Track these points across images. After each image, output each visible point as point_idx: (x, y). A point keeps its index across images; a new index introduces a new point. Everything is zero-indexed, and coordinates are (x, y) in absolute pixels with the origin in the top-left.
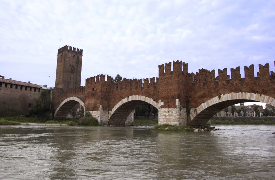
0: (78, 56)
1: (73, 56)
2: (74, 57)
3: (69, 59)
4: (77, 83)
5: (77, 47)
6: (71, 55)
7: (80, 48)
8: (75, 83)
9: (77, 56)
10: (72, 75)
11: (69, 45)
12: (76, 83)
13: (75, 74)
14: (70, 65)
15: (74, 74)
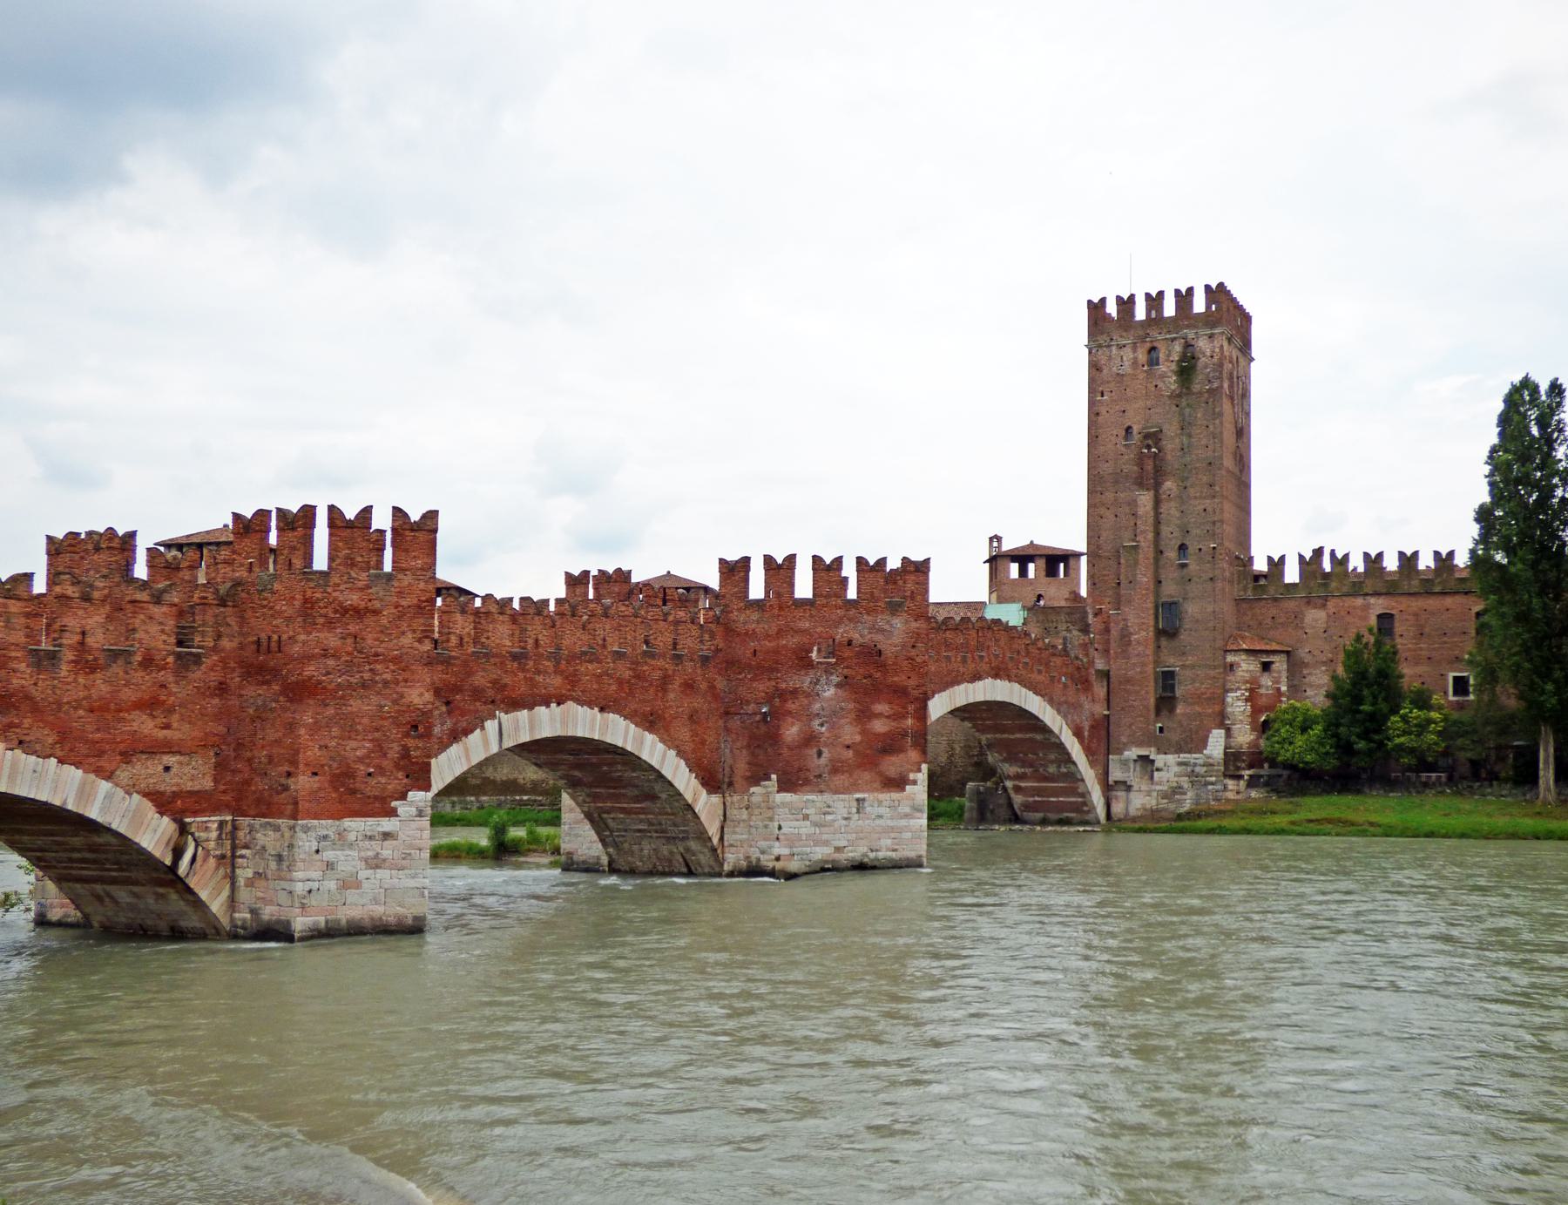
0: (1187, 345)
1: (1142, 356)
2: (1153, 362)
3: (1171, 378)
4: (1192, 549)
5: (1169, 284)
6: (1128, 354)
7: (1198, 280)
8: (1171, 554)
9: (1178, 348)
10: (1145, 499)
11: (1109, 293)
12: (1182, 548)
13: (1169, 485)
14: (1128, 430)
15: (1157, 486)
